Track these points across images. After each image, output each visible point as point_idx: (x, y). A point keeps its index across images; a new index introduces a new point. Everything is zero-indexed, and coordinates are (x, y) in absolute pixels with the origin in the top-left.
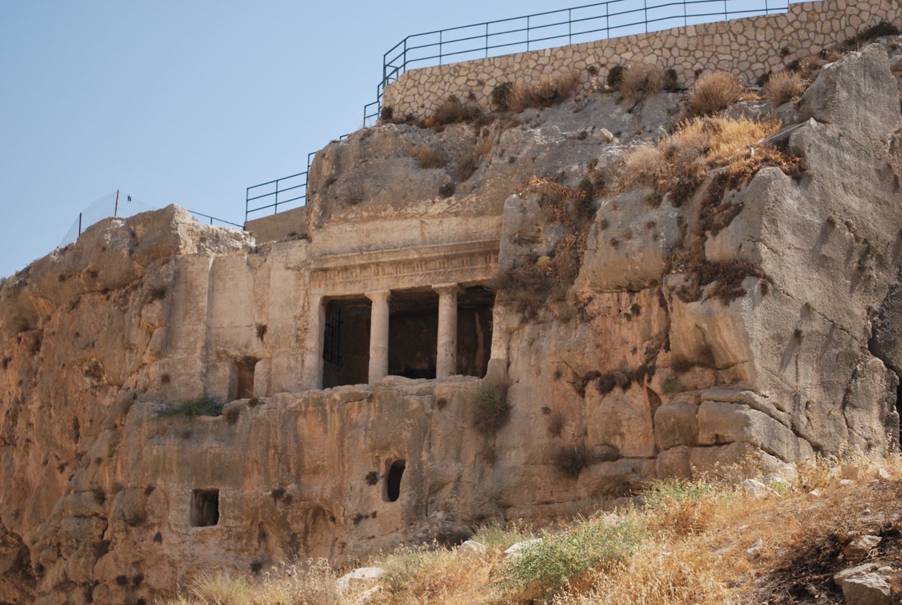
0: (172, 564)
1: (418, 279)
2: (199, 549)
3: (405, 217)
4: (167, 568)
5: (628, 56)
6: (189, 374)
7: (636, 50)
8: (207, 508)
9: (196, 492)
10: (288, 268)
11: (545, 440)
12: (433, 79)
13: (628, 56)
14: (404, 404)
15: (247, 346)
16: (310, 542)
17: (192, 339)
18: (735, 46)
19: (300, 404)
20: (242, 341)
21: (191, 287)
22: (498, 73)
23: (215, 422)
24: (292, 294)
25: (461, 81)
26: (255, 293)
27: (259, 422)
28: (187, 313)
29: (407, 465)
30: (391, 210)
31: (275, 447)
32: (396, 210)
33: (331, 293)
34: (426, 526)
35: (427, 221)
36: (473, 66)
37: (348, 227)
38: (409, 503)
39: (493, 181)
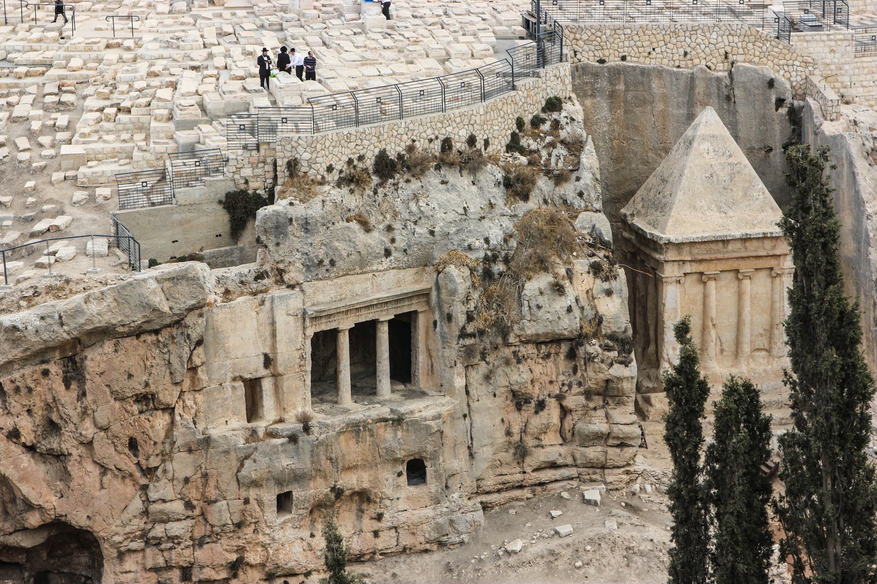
0: (264, 546)
1: (371, 316)
2: (281, 533)
3: (365, 273)
4: (259, 549)
5: (449, 129)
6: (223, 399)
7: (455, 125)
8: (284, 502)
9: (279, 497)
10: (288, 315)
11: (503, 440)
12: (334, 144)
13: (449, 129)
14: (428, 427)
15: (256, 371)
16: (341, 511)
17: (223, 372)
18: (500, 119)
19: (343, 428)
20: (252, 367)
21: (218, 332)
22: (374, 140)
23: (282, 444)
24: (293, 333)
25: (352, 145)
26: (259, 331)
27: (321, 443)
28: (216, 352)
29: (427, 464)
30: (358, 270)
31: (331, 459)
32: (361, 269)
33: (318, 329)
34: (448, 504)
35: (377, 274)
36: (358, 134)
37: (329, 282)
38: (437, 491)
39: (420, 247)
